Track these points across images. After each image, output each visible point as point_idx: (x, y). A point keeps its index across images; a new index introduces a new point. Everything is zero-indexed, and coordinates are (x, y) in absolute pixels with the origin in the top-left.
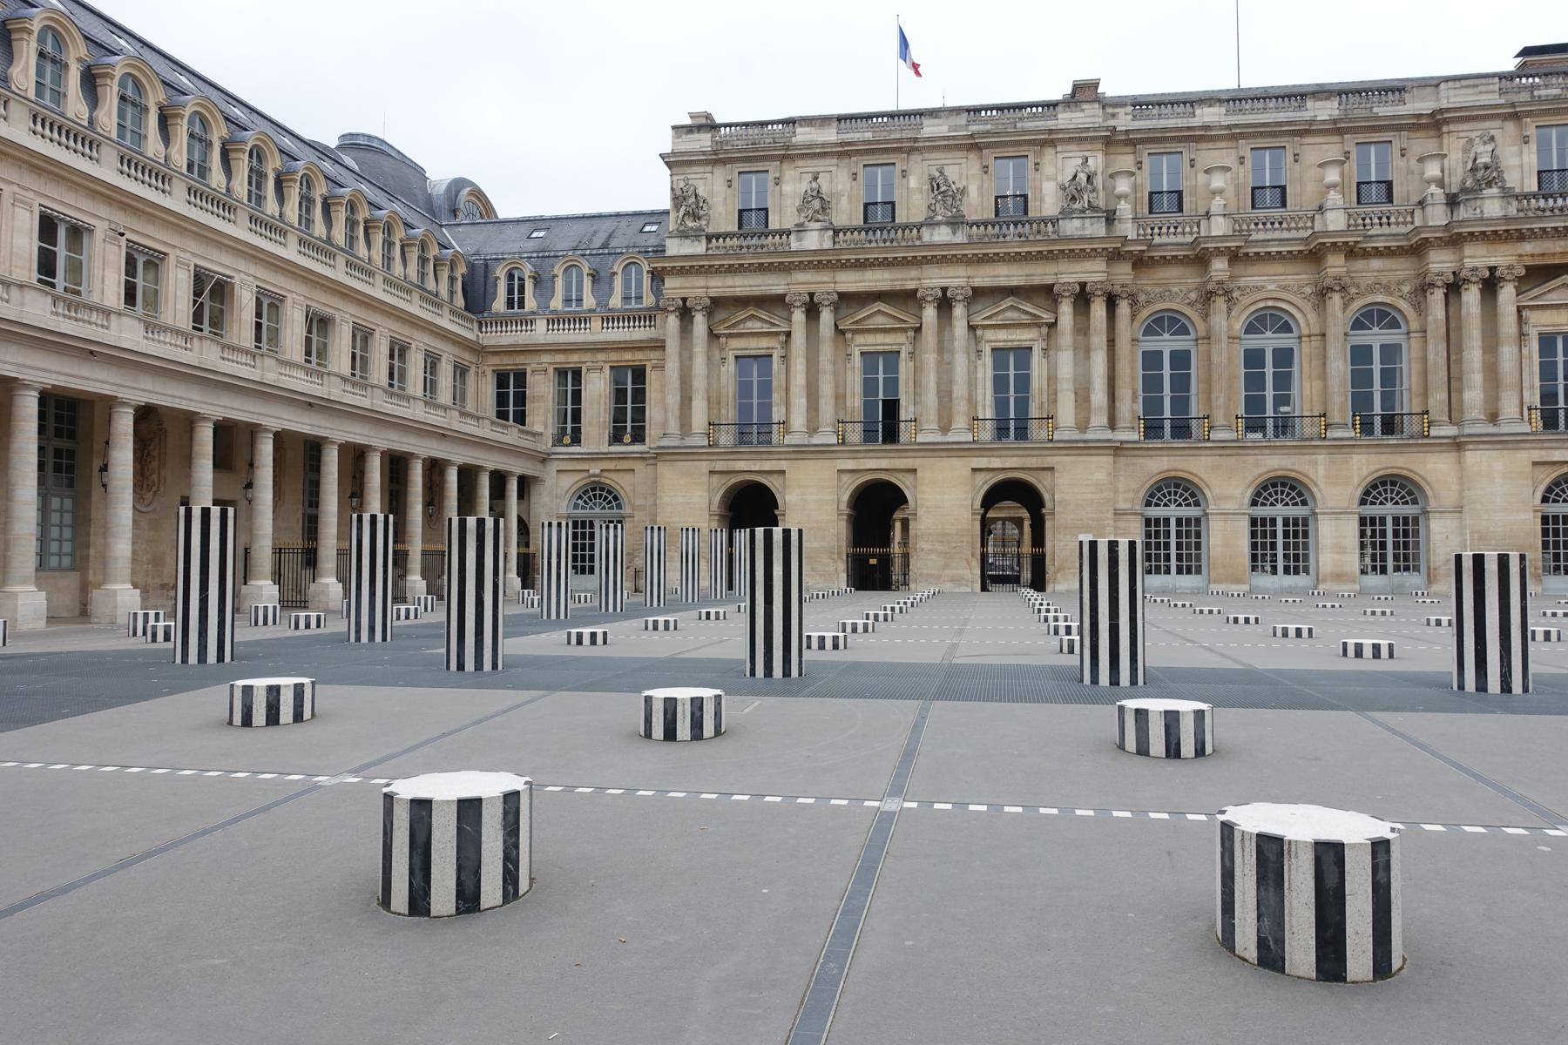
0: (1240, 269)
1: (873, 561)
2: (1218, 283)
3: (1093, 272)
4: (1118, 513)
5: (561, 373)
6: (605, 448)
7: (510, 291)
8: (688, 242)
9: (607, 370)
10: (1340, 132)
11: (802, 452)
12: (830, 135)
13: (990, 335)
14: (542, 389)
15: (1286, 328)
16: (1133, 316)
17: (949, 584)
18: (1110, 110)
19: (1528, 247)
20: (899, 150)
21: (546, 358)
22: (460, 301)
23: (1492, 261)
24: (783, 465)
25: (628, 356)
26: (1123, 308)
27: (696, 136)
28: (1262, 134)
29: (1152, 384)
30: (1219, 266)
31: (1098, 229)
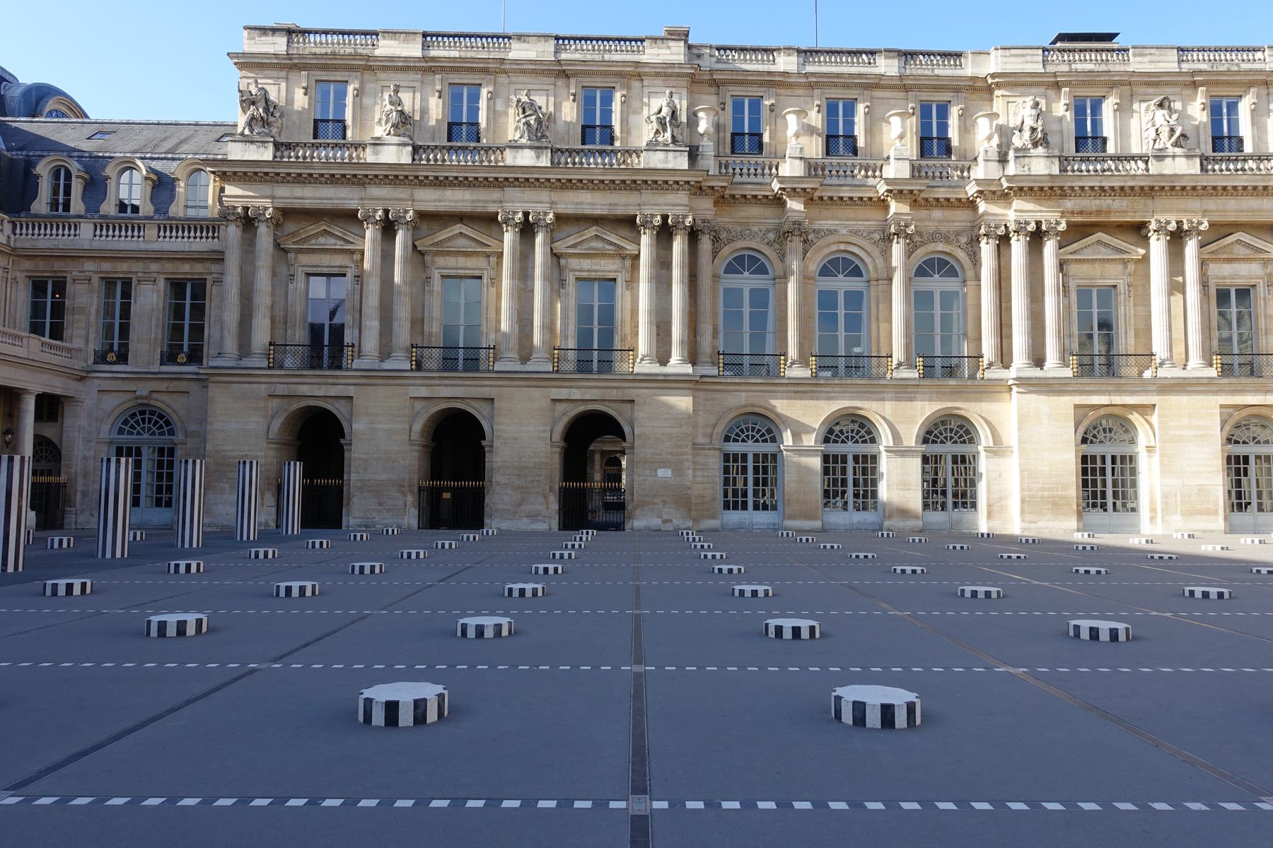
0: (815, 211)
1: (447, 495)
2: (794, 223)
3: (676, 205)
4: (695, 446)
5: (109, 283)
6: (156, 367)
7: (55, 192)
8: (253, 147)
9: (161, 284)
10: (906, 88)
11: (371, 377)
12: (413, 50)
13: (574, 263)
14: (85, 301)
15: (857, 272)
16: (715, 253)
17: (525, 520)
18: (695, 51)
19: (1069, 204)
20: (485, 71)
21: (90, 266)
23: (1039, 216)
24: (351, 391)
25: (186, 268)
26: (705, 244)
27: (270, 39)
28: (836, 85)
29: (733, 317)
30: (795, 205)
31: (682, 162)
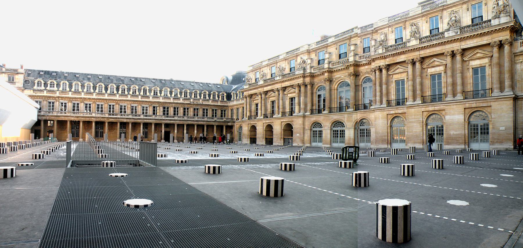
13: (289, 95)
22: (225, 99)
